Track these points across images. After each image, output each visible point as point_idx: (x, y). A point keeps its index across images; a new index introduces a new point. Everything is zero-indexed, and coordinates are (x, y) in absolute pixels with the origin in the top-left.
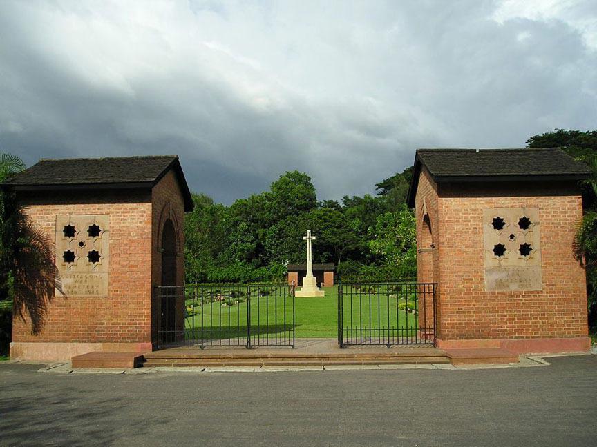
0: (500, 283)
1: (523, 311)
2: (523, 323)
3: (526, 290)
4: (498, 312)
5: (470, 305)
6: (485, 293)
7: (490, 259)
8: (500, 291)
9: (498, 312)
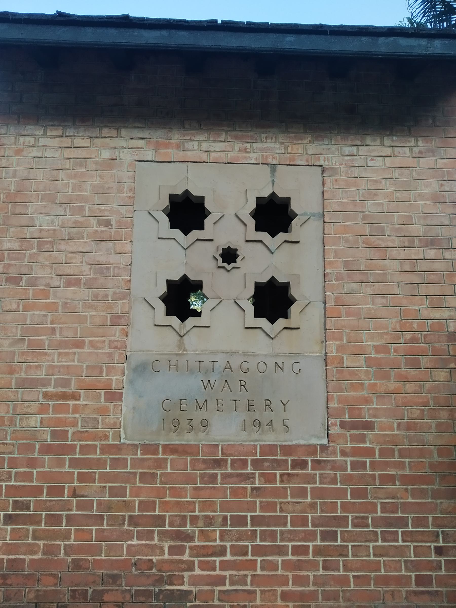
0: (176, 414)
1: (256, 521)
2: (252, 565)
3: (270, 439)
4: (160, 521)
5: (60, 491)
6: (118, 448)
7: (150, 329)
9: (160, 521)
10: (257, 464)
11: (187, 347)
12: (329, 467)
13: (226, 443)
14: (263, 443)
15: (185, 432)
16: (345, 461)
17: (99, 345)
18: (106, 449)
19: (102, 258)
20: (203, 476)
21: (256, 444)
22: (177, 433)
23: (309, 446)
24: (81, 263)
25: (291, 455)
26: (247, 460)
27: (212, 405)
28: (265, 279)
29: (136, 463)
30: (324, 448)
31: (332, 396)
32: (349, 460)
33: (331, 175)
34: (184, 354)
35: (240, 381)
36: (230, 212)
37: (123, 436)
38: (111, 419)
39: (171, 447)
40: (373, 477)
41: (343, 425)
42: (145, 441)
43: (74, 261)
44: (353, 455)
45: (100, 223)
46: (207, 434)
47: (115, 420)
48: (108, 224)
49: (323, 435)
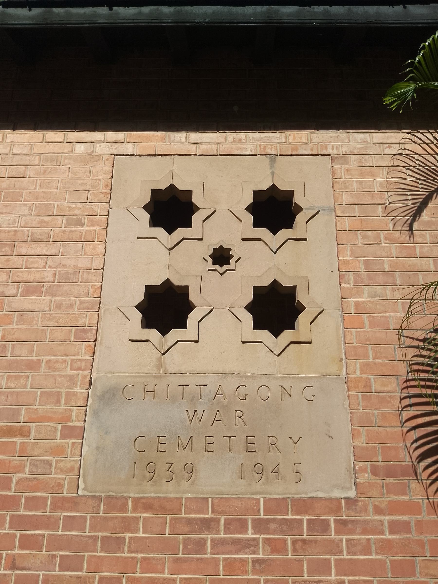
0: (152, 456)
3: (278, 490)
6: (73, 503)
8: (150, 492)
10: (261, 526)
11: (167, 366)
12: (359, 530)
13: (218, 496)
14: (268, 496)
15: (164, 480)
16: (380, 521)
17: (58, 366)
18: (58, 504)
19: (70, 262)
20: (186, 542)
21: (258, 497)
22: (153, 482)
23: (330, 499)
24: (44, 268)
25: (306, 513)
26: (246, 520)
27: (199, 443)
28: (265, 283)
29: (98, 524)
30: (351, 502)
31: (359, 431)
32: (386, 519)
33: (342, 165)
34: (165, 376)
35: (236, 411)
36: (222, 208)
37: (81, 485)
38: (68, 462)
39: (144, 501)
40: (421, 544)
41: (375, 471)
42: (111, 493)
43: (36, 266)
44: (391, 513)
45: (69, 223)
46: (193, 483)
47: (72, 463)
48: (79, 223)
49: (348, 485)
